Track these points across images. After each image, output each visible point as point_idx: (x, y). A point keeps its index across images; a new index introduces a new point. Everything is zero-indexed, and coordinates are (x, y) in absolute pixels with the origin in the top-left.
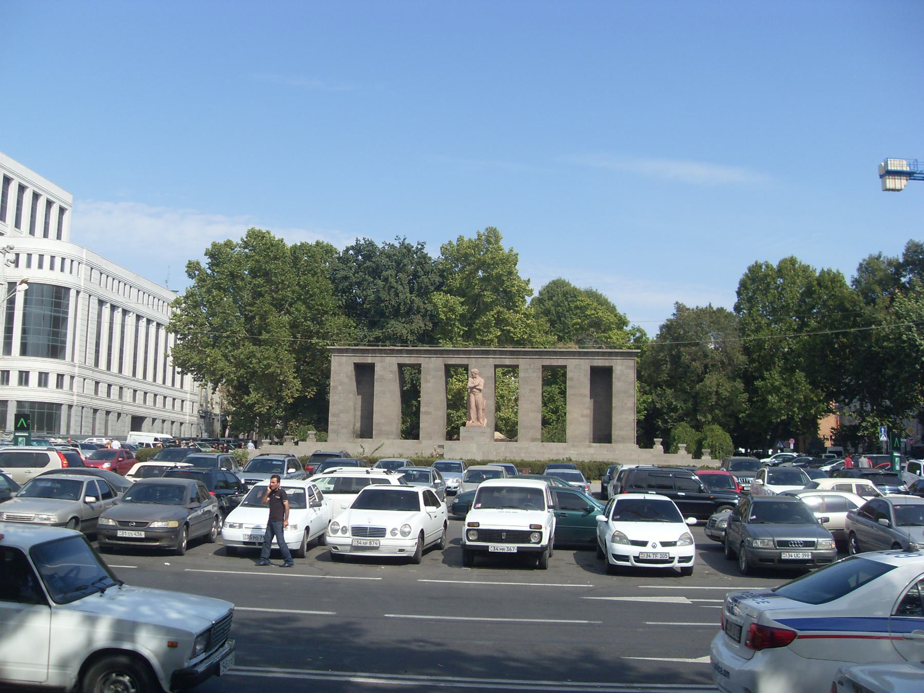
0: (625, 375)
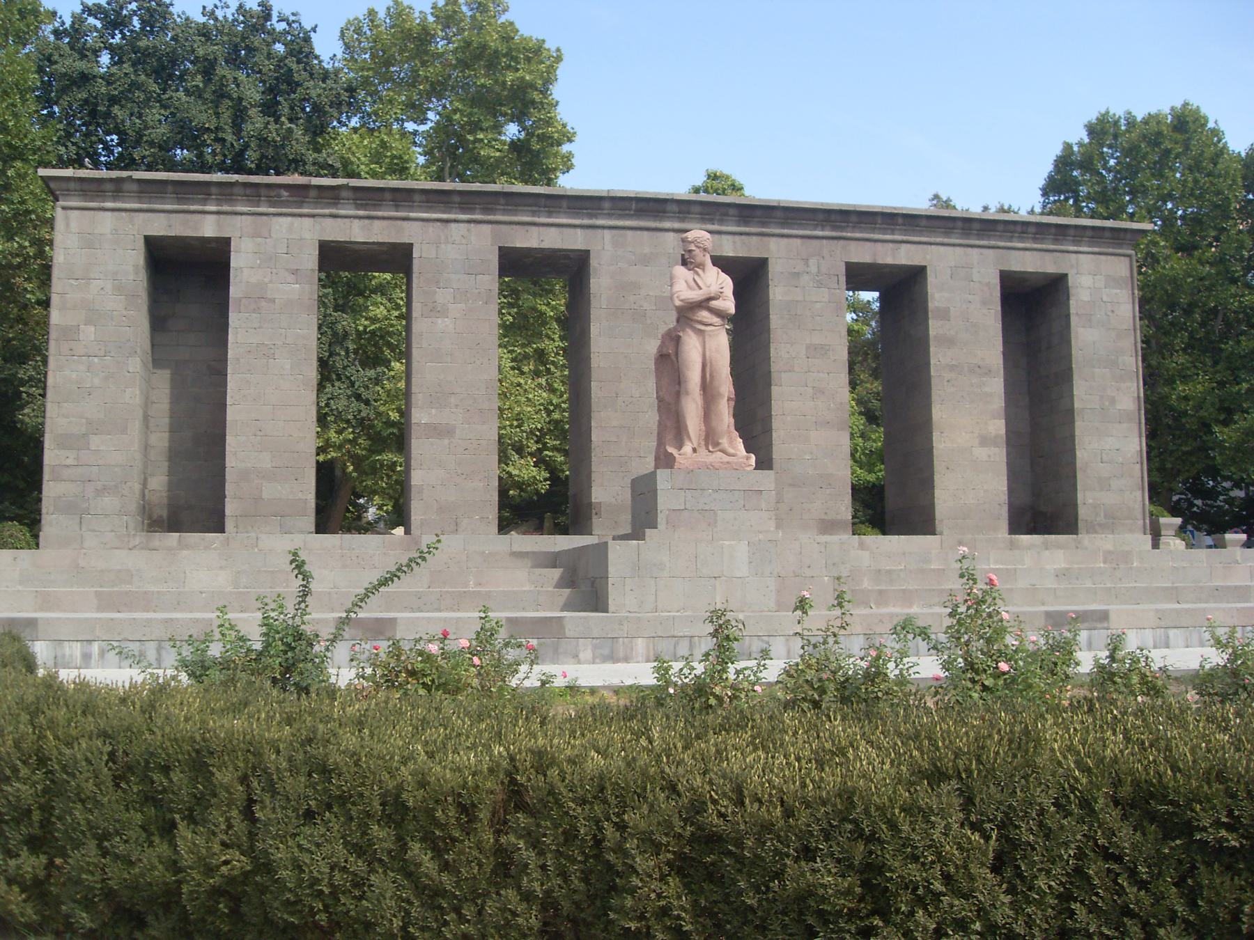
0: (1103, 304)
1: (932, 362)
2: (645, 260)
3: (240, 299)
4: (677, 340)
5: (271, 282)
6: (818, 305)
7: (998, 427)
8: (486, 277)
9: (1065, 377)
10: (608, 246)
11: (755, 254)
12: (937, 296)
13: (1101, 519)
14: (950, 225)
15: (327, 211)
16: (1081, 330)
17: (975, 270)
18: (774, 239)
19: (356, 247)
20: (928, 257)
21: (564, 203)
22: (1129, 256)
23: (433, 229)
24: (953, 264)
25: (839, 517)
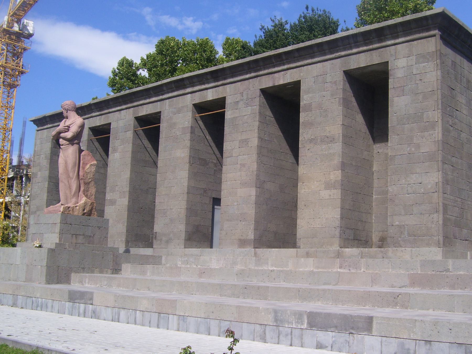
2: (179, 111)
6: (246, 117)
16: (396, 99)
17: (328, 75)
20: (302, 74)
22: (434, 36)
24: (315, 74)
25: (248, 238)
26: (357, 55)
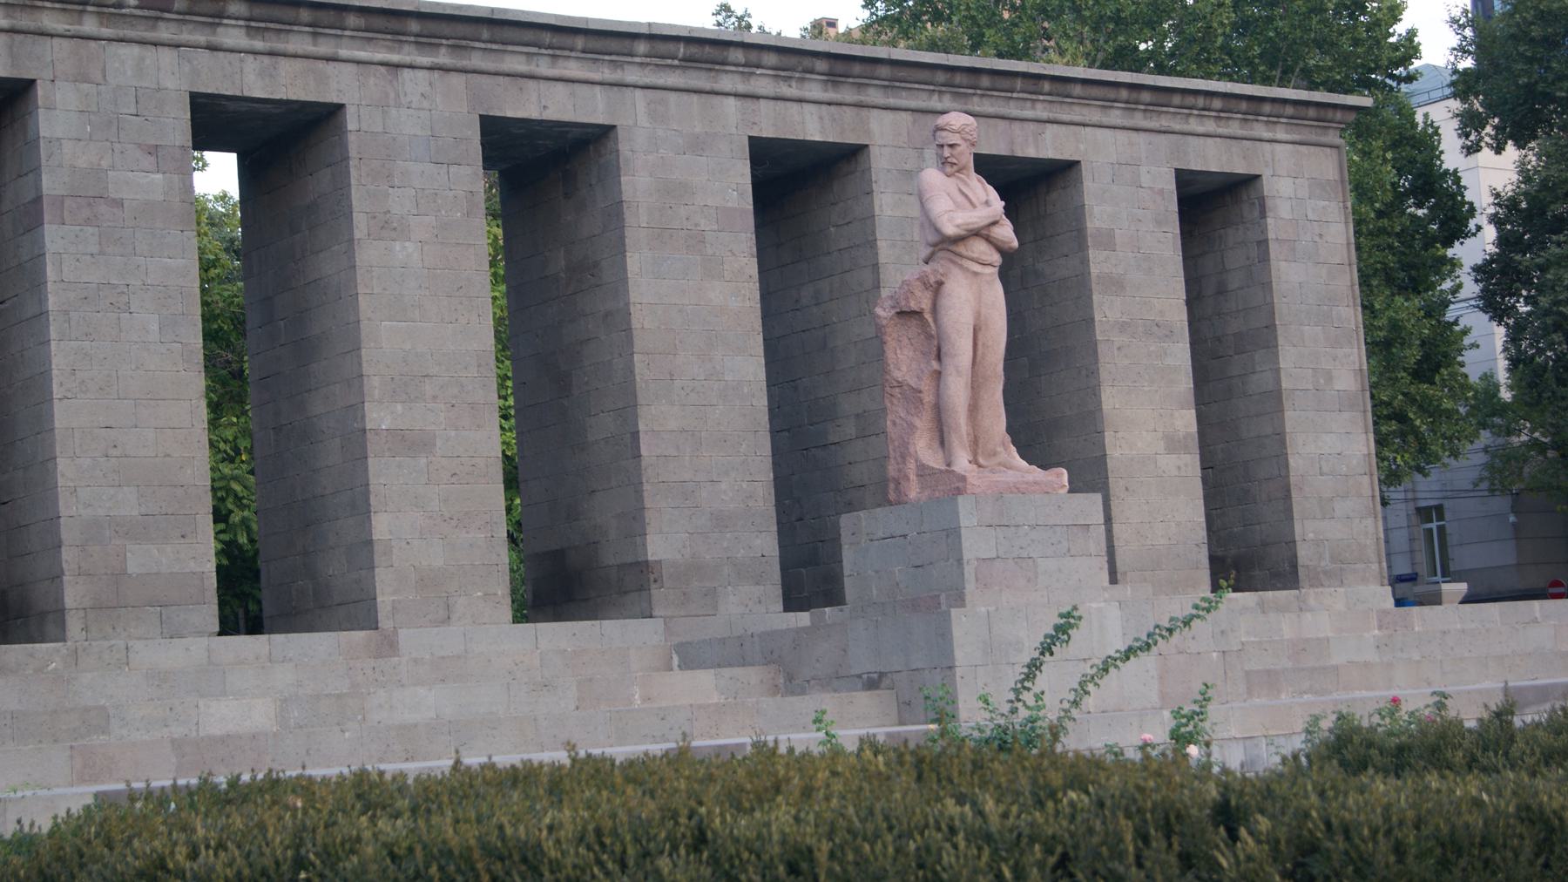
1: (1097, 317)
2: (697, 145)
3: (61, 200)
4: (937, 288)
5: (113, 167)
7: (1186, 421)
8: (465, 171)
9: (1265, 337)
10: (643, 120)
11: (852, 139)
12: (1096, 210)
13: (1326, 563)
14: (1111, 93)
15: (201, 38)
16: (1283, 264)
17: (1143, 169)
18: (875, 112)
19: (232, 106)
20: (1082, 147)
21: (580, 42)
23: (377, 81)
26: (1202, 139)
